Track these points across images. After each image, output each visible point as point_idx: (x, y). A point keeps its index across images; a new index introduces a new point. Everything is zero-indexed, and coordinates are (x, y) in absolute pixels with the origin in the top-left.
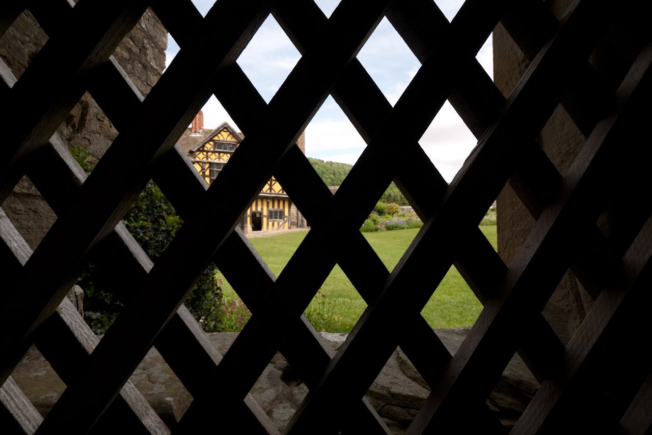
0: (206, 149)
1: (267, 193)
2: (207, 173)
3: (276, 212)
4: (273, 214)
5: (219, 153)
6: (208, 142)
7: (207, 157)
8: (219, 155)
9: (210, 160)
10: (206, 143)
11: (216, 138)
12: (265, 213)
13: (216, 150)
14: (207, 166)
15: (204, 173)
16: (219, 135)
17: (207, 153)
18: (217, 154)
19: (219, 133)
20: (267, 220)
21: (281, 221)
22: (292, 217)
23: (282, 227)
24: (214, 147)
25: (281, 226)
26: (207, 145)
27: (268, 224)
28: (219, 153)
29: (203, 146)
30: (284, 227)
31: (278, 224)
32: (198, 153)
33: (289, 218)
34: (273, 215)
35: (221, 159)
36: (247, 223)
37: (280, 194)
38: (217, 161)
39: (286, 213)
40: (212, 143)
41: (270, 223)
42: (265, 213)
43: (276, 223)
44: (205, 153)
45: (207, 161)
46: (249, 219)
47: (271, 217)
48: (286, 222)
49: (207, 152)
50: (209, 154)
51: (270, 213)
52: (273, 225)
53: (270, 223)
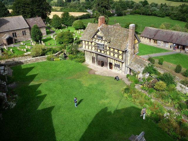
2: (96, 46)
3: (117, 65)
5: (99, 39)
11: (97, 34)
12: (113, 64)
14: (96, 43)
19: (98, 32)
22: (123, 68)
26: (95, 36)
31: (118, 69)
34: (116, 65)
36: (107, 65)
38: (98, 42)
39: (121, 67)
40: (96, 36)
41: (115, 68)
43: (117, 69)
46: (108, 64)
47: (115, 66)
52: (116, 69)
53: (115, 68)
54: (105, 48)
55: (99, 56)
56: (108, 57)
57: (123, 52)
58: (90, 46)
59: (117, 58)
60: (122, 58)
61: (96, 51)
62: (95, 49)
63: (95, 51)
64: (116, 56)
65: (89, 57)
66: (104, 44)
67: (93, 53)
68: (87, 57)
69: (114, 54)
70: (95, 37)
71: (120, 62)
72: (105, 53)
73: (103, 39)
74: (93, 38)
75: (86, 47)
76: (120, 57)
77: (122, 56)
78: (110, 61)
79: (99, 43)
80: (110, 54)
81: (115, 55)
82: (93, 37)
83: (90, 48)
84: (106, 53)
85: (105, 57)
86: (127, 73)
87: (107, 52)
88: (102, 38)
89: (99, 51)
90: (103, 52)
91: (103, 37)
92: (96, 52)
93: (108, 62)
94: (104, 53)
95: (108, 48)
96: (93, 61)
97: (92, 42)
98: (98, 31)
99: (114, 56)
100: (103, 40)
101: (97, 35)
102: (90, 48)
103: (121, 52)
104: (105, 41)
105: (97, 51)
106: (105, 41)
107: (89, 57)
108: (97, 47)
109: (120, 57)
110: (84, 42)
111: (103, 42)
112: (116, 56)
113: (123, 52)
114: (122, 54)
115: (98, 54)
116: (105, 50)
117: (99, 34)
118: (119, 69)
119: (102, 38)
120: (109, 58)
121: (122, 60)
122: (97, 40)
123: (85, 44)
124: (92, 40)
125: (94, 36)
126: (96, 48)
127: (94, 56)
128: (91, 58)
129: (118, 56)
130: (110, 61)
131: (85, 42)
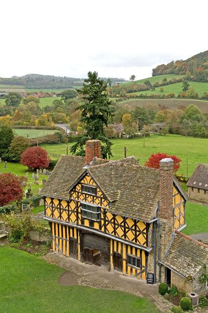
0: (77, 190)
1: (121, 239)
2: (79, 211)
3: (134, 259)
5: (86, 194)
6: (77, 184)
9: (80, 200)
10: (76, 186)
11: (82, 182)
12: (124, 257)
15: (77, 210)
16: (84, 179)
19: (84, 177)
23: (139, 276)
25: (138, 274)
26: (77, 187)
27: (127, 269)
30: (141, 276)
31: (136, 271)
32: (72, 192)
33: (146, 269)
34: (130, 260)
36: (109, 260)
37: (134, 243)
38: (83, 202)
39: (144, 263)
40: (80, 185)
41: (129, 268)
42: (124, 257)
43: (134, 270)
46: (111, 257)
47: (130, 263)
48: (142, 272)
50: (80, 194)
51: (128, 257)
52: (131, 270)
53: (129, 268)
54: (102, 217)
55: (88, 239)
56: (109, 239)
57: (148, 225)
58: (65, 210)
59: (134, 241)
60: (147, 242)
62: (78, 217)
63: (78, 224)
64: (130, 235)
65: (61, 240)
66: (99, 205)
67: (73, 228)
68: (57, 239)
70: (78, 188)
71: (141, 250)
72: (103, 229)
73: (96, 194)
74: (72, 190)
75: (55, 213)
76: (141, 239)
77: (145, 235)
78: (115, 250)
79: (87, 203)
80: (115, 232)
81: (127, 234)
82: (74, 189)
83: (65, 215)
84: (106, 228)
85: (104, 238)
86: (160, 281)
87: (107, 227)
88: (94, 191)
89: (87, 223)
90: (96, 226)
91: (98, 190)
92: (79, 227)
93: (111, 252)
94: (100, 228)
95: (109, 216)
96: (73, 251)
97: (68, 202)
98: (86, 174)
99: (125, 235)
100: (97, 197)
101: (81, 184)
102: (65, 215)
103: (142, 226)
104: (103, 200)
105: (83, 223)
106: (101, 199)
107: (61, 240)
108: (81, 213)
109: (141, 239)
110: (49, 201)
111: (97, 201)
112: (130, 235)
113: (148, 225)
114: (145, 231)
115: (82, 233)
116: (103, 222)
117: (87, 181)
118: (138, 271)
119: (94, 191)
120: (113, 240)
121: (145, 245)
122: (82, 197)
123: (52, 207)
124: (71, 197)
125: (75, 187)
126: (80, 215)
127: (75, 237)
128: (68, 242)
129: (136, 236)
130: (115, 250)
131: (52, 202)
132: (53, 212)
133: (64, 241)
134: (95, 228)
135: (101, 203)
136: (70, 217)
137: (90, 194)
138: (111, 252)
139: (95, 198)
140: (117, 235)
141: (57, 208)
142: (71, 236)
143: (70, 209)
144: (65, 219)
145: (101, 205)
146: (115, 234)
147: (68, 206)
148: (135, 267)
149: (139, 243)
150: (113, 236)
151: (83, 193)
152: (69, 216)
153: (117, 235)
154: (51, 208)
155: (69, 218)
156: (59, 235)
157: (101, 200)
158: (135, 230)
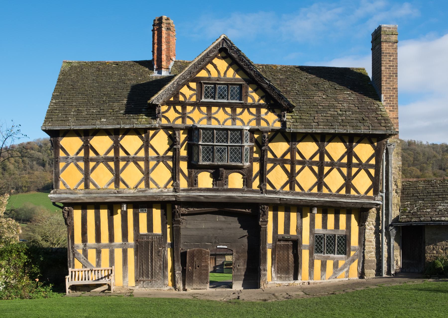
4: (325, 242)
7: (184, 116)
8: (209, 110)
9: (189, 123)
12: (306, 240)
13: (203, 100)
17: (184, 108)
18: (204, 109)
20: (311, 255)
21: (342, 259)
23: (343, 273)
24: (199, 94)
25: (342, 269)
28: (209, 106)
29: (176, 94)
30: (347, 272)
31: (336, 265)
35: (213, 120)
39: (354, 241)
40: (193, 85)
41: (318, 264)
42: (306, 240)
43: (330, 264)
44: (179, 108)
45: (183, 126)
48: (353, 261)
49: (184, 105)
50: (189, 108)
52: (324, 266)
53: (318, 264)
58: (135, 160)
60: (375, 187)
61: (183, 183)
63: (176, 189)
66: (253, 124)
69: (320, 176)
72: (256, 184)
77: (372, 171)
78: (281, 231)
93: (270, 240)
99: (320, 184)
100: (245, 106)
101: (198, 81)
106: (258, 107)
114: (373, 162)
121: (371, 194)
123: (87, 160)
130: (281, 231)
132: (87, 173)
133: (118, 253)
134: (229, 187)
135: (258, 118)
136: (152, 175)
137: (225, 101)
138: (270, 240)
139: (239, 110)
140: (297, 189)
141: (106, 160)
142: (143, 230)
143: (152, 154)
144: (132, 184)
145: (258, 123)
146: (292, 188)
147: (147, 145)
148: (332, 255)
149: (356, 194)
150: (287, 193)
151: (204, 104)
152: (147, 173)
153: (297, 189)
154: (82, 164)
155: (147, 178)
156: (98, 238)
157: (259, 112)
158: (349, 165)
